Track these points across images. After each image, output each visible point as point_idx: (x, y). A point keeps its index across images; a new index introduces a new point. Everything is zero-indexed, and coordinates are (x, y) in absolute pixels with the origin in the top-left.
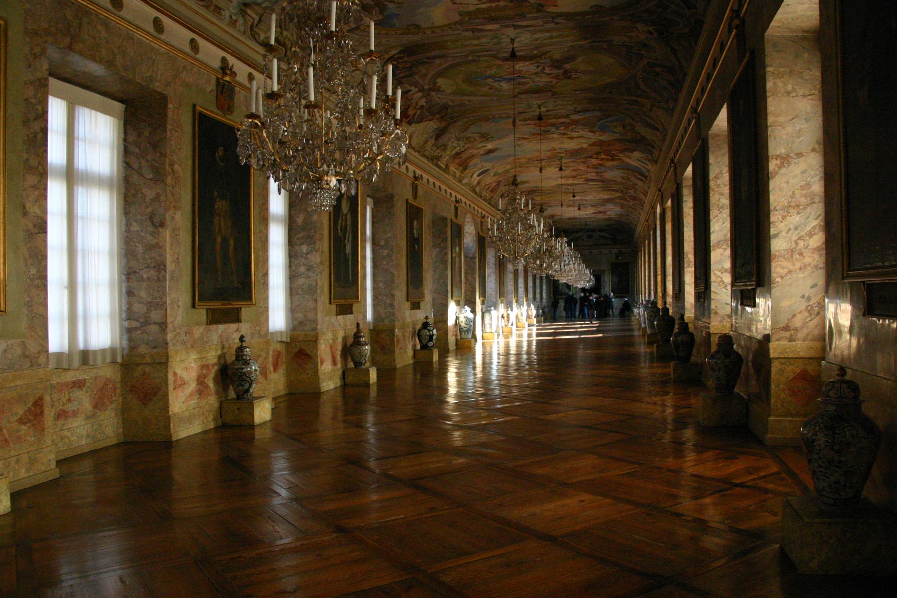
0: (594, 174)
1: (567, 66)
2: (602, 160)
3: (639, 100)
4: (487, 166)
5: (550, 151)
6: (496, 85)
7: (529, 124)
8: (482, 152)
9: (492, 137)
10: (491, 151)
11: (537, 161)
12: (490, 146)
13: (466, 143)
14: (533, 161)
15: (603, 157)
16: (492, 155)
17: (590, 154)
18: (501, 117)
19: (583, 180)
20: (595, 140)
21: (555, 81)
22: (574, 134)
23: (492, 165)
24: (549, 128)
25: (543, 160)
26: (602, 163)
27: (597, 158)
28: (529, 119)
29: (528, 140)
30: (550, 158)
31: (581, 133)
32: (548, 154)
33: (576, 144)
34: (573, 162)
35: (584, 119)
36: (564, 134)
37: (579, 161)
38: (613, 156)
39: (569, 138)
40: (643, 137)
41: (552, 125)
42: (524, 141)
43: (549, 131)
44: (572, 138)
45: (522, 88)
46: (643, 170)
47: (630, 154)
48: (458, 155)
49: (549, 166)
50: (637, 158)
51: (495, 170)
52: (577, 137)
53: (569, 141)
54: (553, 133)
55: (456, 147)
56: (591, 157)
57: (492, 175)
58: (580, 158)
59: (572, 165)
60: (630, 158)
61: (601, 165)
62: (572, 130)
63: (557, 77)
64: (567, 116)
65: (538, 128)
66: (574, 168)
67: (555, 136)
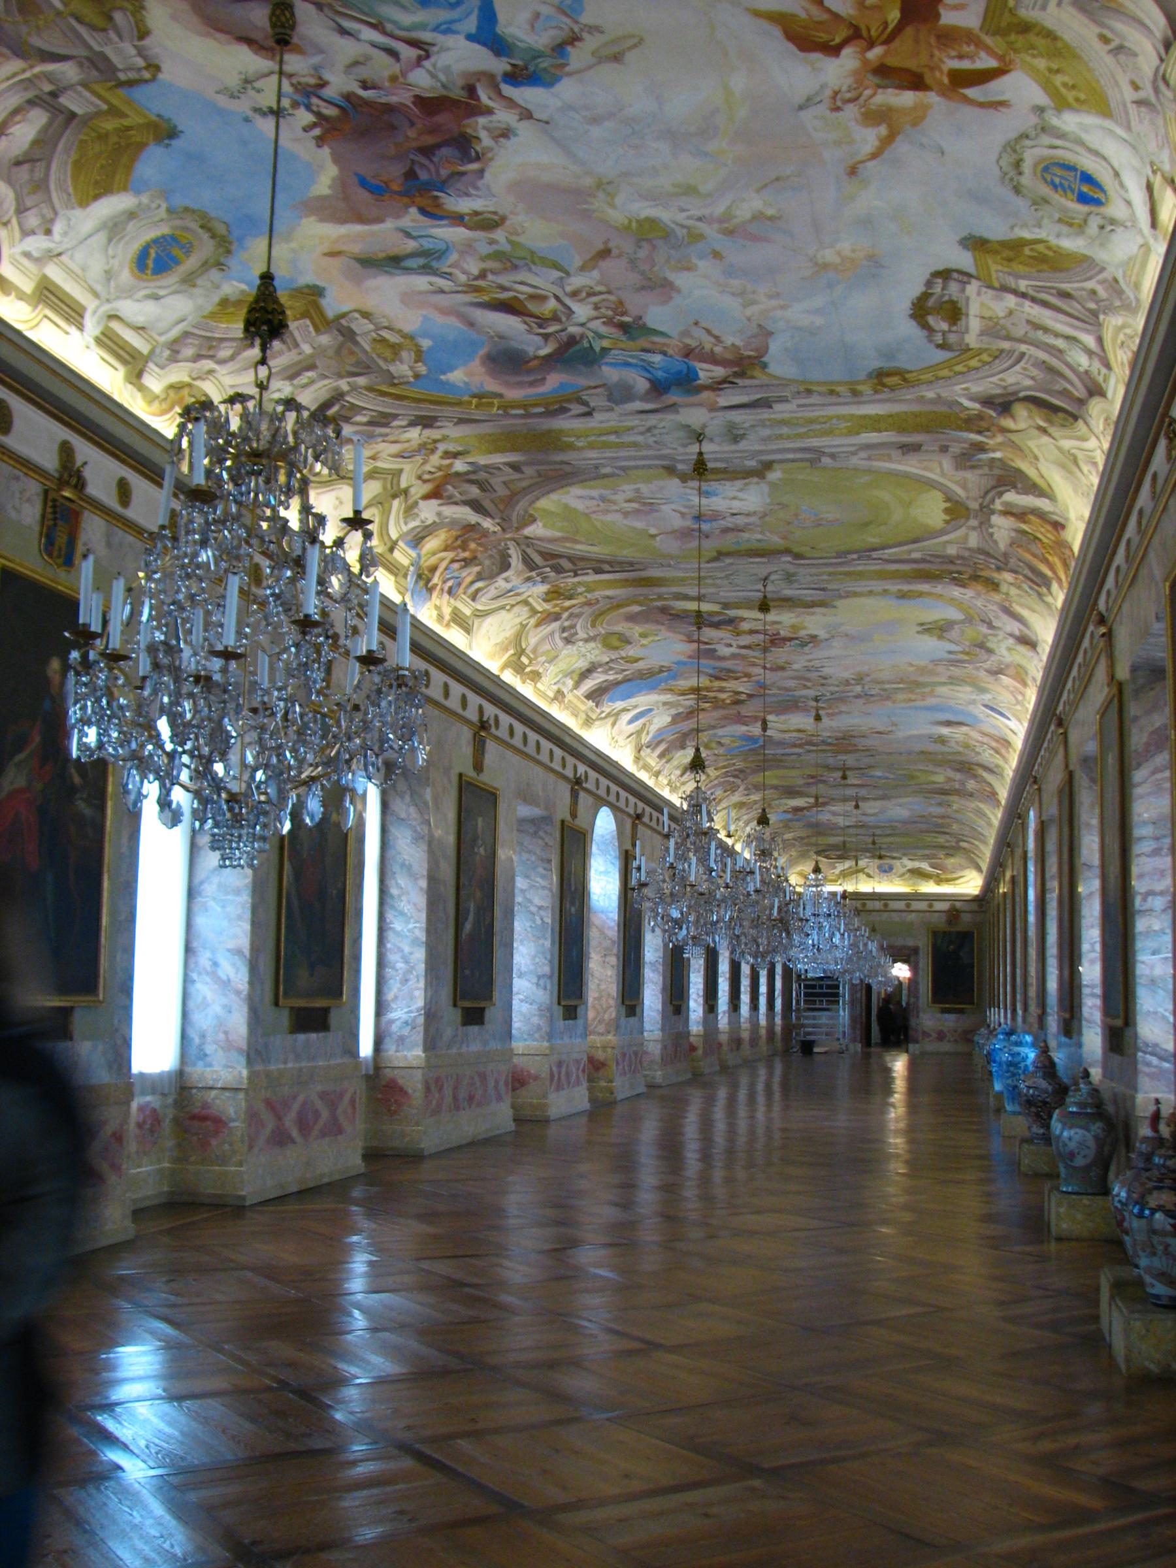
0: (724, 651)
2: (722, 690)
5: (841, 712)
14: (880, 695)
17: (755, 701)
19: (745, 626)
22: (795, 734)
25: (858, 697)
26: (717, 684)
30: (842, 700)
31: (787, 736)
34: (786, 689)
37: (775, 691)
41: (830, 744)
44: (799, 731)
46: (619, 705)
47: (673, 711)
49: (847, 683)
53: (802, 727)
56: (750, 696)
58: (774, 695)
59: (792, 684)
64: (810, 751)
66: (780, 674)
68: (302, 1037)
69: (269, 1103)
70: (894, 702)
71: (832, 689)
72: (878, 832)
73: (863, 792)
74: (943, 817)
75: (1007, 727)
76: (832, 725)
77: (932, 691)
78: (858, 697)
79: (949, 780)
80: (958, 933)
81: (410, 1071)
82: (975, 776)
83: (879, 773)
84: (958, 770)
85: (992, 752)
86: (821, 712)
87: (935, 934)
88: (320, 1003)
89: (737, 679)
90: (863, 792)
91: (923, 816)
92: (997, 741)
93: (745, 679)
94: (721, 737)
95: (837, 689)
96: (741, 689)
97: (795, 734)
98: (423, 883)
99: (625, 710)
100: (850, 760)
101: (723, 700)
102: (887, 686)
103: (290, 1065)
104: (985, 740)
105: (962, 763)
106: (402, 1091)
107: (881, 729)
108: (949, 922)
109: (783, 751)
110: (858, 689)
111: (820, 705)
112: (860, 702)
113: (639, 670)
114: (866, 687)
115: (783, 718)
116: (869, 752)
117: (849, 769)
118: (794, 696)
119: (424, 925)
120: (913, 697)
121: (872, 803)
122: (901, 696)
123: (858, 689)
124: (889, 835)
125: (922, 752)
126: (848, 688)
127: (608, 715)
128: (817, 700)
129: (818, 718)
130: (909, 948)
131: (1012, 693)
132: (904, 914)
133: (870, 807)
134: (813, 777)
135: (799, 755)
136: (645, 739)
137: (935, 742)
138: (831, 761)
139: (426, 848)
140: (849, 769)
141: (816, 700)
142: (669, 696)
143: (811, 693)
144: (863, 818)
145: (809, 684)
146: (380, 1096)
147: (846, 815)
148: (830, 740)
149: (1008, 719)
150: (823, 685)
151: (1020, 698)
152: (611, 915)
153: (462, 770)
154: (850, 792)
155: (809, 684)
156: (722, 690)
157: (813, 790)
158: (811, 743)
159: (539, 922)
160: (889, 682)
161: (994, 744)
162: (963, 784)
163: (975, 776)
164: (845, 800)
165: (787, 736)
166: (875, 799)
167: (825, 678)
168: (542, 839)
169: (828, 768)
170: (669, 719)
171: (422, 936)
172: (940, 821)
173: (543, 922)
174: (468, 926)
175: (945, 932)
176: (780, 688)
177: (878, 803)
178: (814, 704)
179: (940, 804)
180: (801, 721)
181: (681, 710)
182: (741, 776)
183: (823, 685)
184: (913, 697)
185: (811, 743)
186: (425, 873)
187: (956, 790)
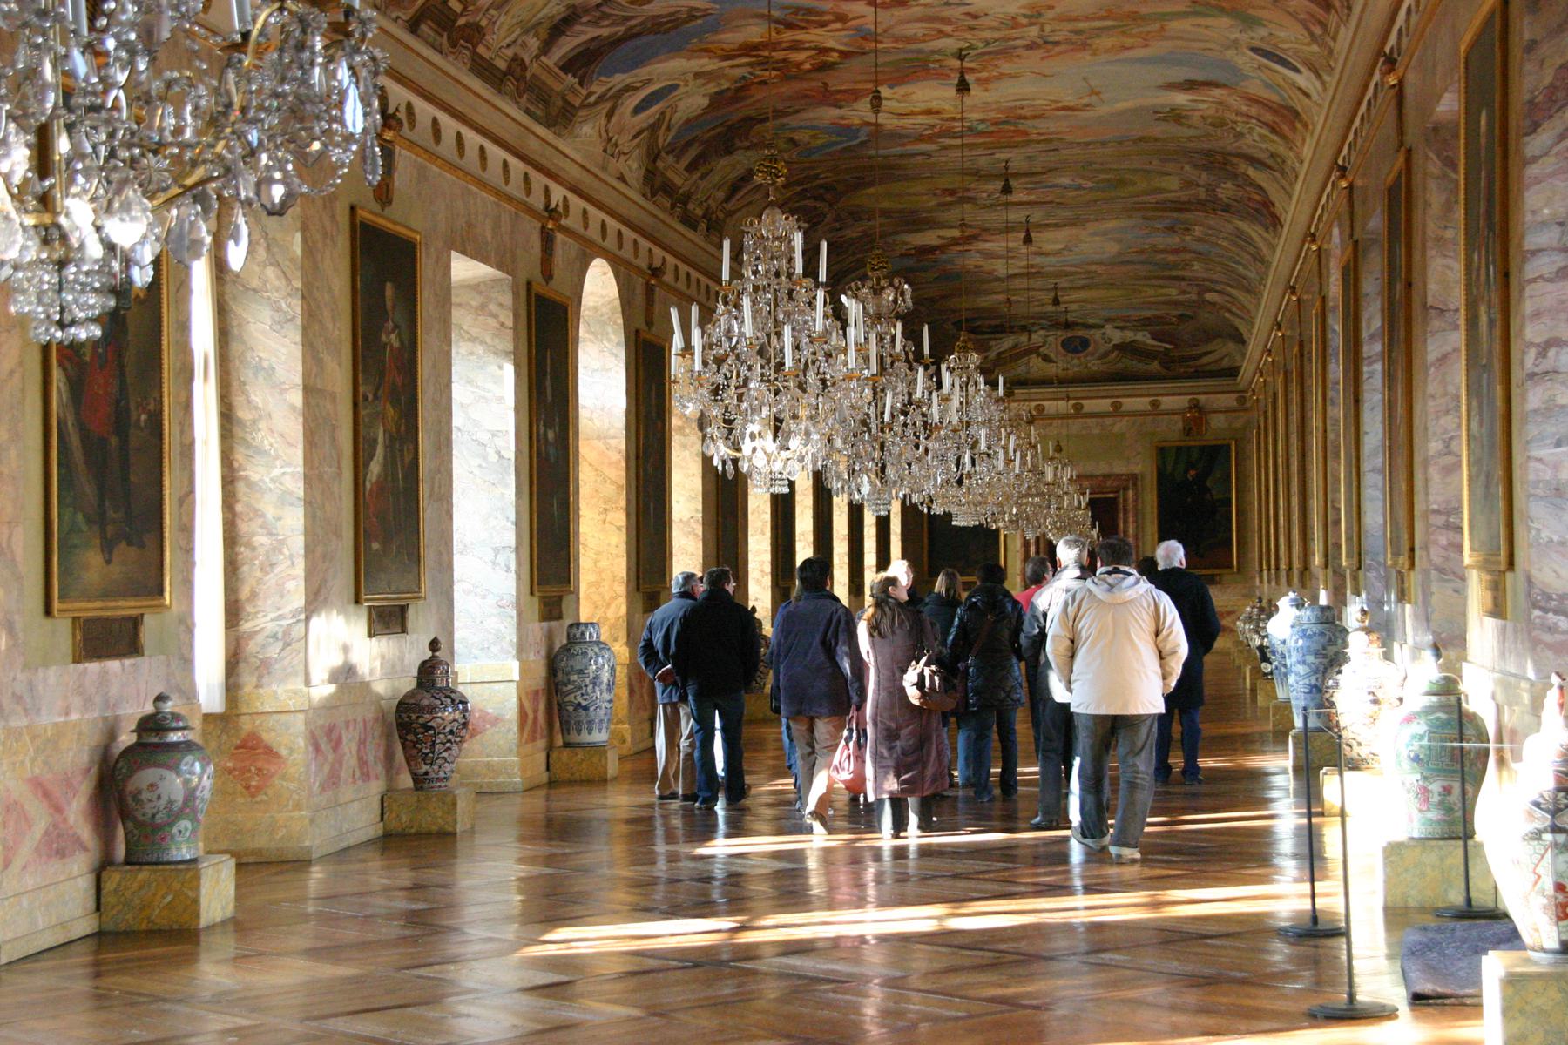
1: (949, 199)
2: (796, 46)
3: (799, 189)
4: (1245, 61)
5: (1001, 77)
6: (1081, 181)
7: (1039, 134)
8: (1218, 92)
9: (1156, 113)
10: (1190, 85)
11: (1057, 43)
12: (1181, 99)
13: (1235, 122)
14: (1068, 41)
15: (800, 56)
16: (1199, 76)
17: (855, 63)
18: (1104, 144)
20: (855, 106)
21: (973, 186)
22: (921, 119)
23: (1230, 54)
24: (992, 129)
25: (1031, 46)
26: (789, 36)
27: (824, 51)
28: (1039, 142)
29: (1060, 105)
31: (905, 122)
32: (1006, 67)
33: (914, 97)
34: (910, 40)
35: (904, 145)
36: (954, 119)
38: (764, 63)
39: (938, 113)
40: (729, 151)
41: (981, 134)
42: (1072, 104)
43: (995, 124)
44: (929, 112)
45: (1034, 179)
46: (620, 80)
47: (712, 88)
48: (1273, 130)
49: (1014, 23)
50: (682, 90)
51: (1236, 35)
52: (912, 113)
53: (934, 105)
54: (983, 121)
55: (1262, 136)
56: (845, 55)
57: (1263, 32)
59: (917, 29)
60: (697, 75)
61: (790, 26)
62: (933, 126)
63: (968, 190)
64: (945, 148)
65: (1021, 127)
67: (976, 116)
68: (93, 667)
69: (38, 785)
70: (1094, 54)
71: (988, 35)
72: (1063, 283)
73: (1037, 215)
74: (1176, 251)
75: (1293, 84)
76: (985, 100)
77: (1162, 28)
78: (1031, 46)
79: (1189, 184)
80: (1202, 449)
81: (284, 717)
82: (1234, 176)
83: (1065, 181)
84: (1204, 167)
85: (1265, 131)
86: (969, 78)
87: (1162, 451)
88: (125, 607)
89: (823, 25)
90: (1037, 215)
91: (1142, 252)
92: (1275, 112)
93: (838, 25)
94: (794, 130)
95: (997, 35)
96: (831, 44)
97: (921, 119)
98: (297, 398)
99: (629, 88)
100: (1016, 159)
101: (800, 64)
102: (1081, 25)
103: (74, 717)
104: (1254, 111)
105: (1210, 153)
106: (270, 753)
107: (1069, 100)
108: (1188, 431)
109: (899, 150)
110: (1033, 32)
111: (966, 64)
112: (1033, 59)
113: (654, 17)
114: (1048, 28)
115: (901, 90)
116: (1052, 143)
117: (1016, 175)
118: (920, 51)
119: (300, 469)
120: (1128, 41)
121: (1050, 234)
122: (1106, 42)
123: (1033, 32)
124: (1082, 288)
125: (1141, 139)
126: (1015, 33)
127: (601, 99)
128: (961, 57)
129: (963, 87)
130: (1118, 476)
131: (1303, 23)
132: (1109, 421)
133: (1050, 240)
134: (952, 192)
135: (928, 155)
136: (664, 139)
137: (1165, 119)
138: (983, 162)
139: (298, 338)
140: (1016, 175)
141: (960, 55)
142: (705, 61)
143: (951, 44)
144: (1038, 260)
145: (948, 29)
146: (230, 765)
147: (1009, 255)
148: (981, 127)
149: (1297, 70)
150: (971, 29)
151: (1318, 31)
152: (613, 442)
153: (353, 199)
154: (1017, 215)
155: (948, 29)
156: (796, 46)
157: (953, 215)
158: (948, 133)
159: (493, 457)
160: (1087, 19)
161: (1268, 117)
162: (1211, 189)
163: (1234, 176)
164: (1008, 229)
165: (905, 122)
166: (1057, 226)
167: (975, 17)
168: (495, 316)
169: (977, 174)
170: (705, 102)
171: (298, 489)
172: (1171, 258)
173: (501, 457)
174: (375, 468)
175: (1179, 449)
176: (896, 39)
177: (1065, 233)
178: (957, 63)
179: (1171, 229)
180: (933, 95)
181: (725, 85)
182: (828, 196)
183: (971, 29)
184: (1128, 41)
185: (948, 133)
186: (298, 380)
187: (1200, 202)
